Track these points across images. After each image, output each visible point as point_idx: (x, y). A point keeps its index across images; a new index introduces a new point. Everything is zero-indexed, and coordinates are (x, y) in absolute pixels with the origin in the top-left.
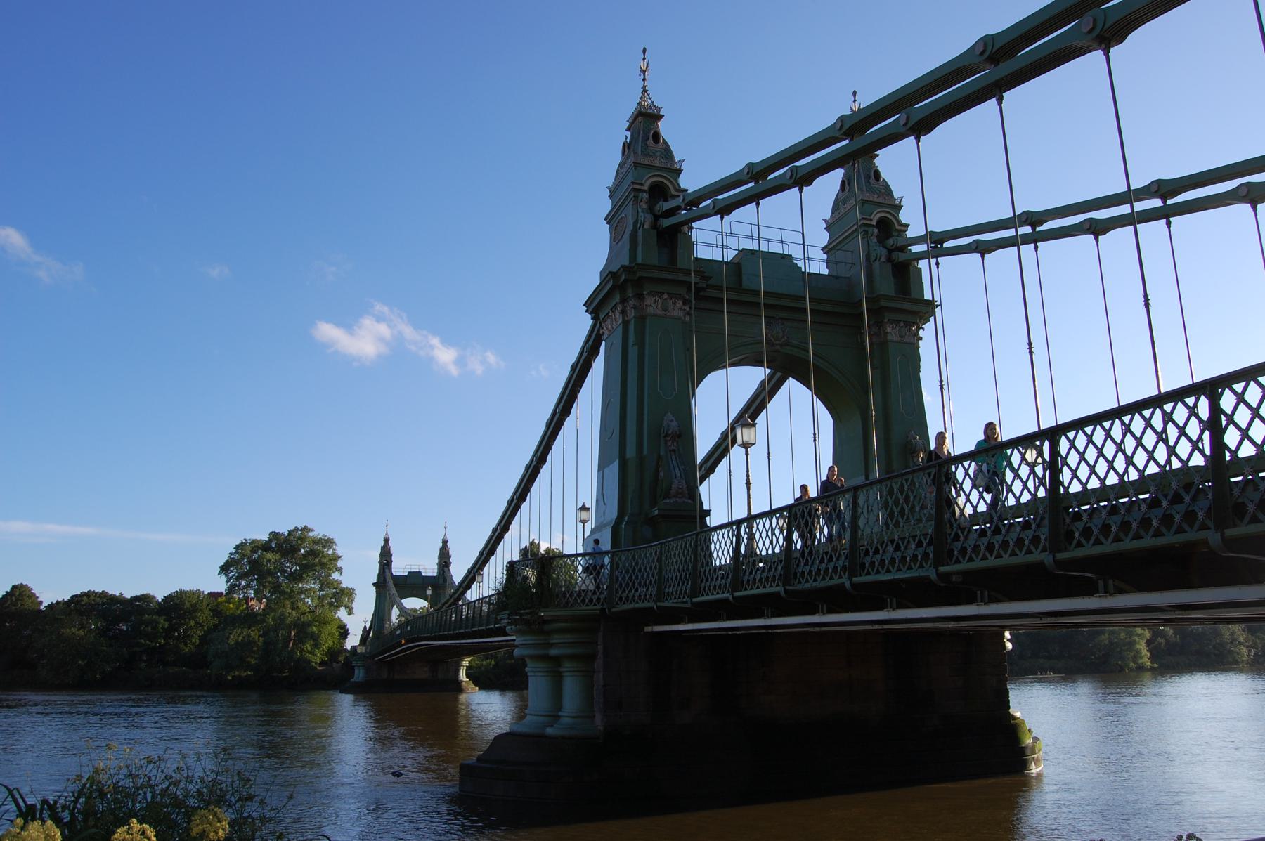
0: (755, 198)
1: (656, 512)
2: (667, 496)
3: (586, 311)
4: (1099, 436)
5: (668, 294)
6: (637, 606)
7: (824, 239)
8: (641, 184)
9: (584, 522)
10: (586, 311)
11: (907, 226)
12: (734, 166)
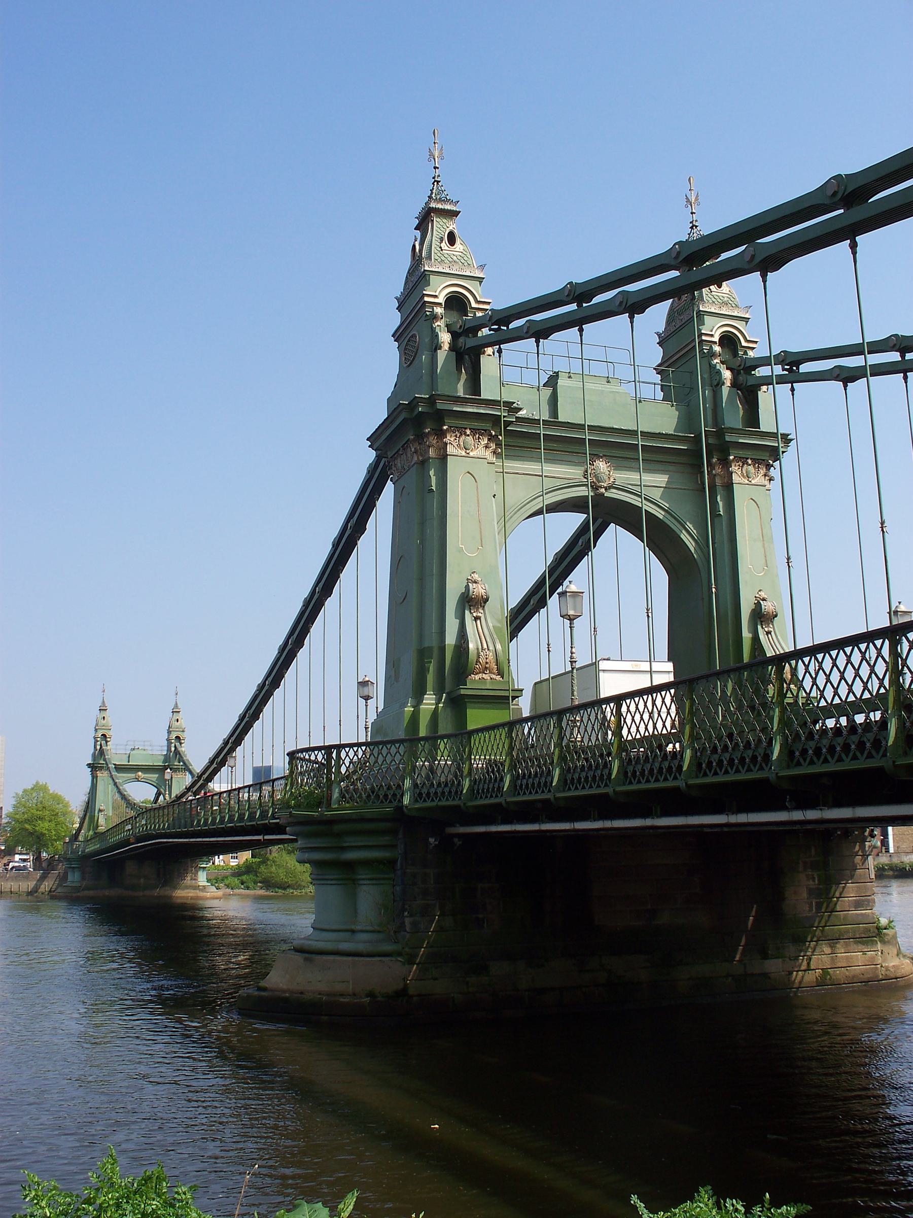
0: (578, 322)
3: (369, 447)
6: (440, 803)
7: (657, 355)
8: (436, 296)
9: (367, 698)
10: (369, 447)
12: (553, 284)
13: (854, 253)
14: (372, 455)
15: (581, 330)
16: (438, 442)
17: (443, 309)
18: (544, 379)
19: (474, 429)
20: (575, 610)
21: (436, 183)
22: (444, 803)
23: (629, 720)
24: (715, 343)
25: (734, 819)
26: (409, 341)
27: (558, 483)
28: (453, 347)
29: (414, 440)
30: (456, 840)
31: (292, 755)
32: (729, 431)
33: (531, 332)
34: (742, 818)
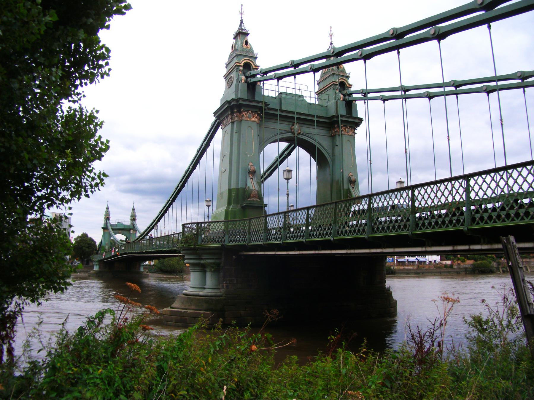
1: (245, 204)
2: (249, 197)
3: (214, 116)
4: (429, 190)
8: (240, 63)
9: (209, 206)
11: (352, 85)
12: (286, 60)
13: (399, 55)
14: (214, 119)
15: (295, 77)
22: (239, 243)
24: (337, 85)
25: (349, 251)
28: (246, 81)
29: (230, 114)
30: (242, 257)
31: (184, 226)
33: (276, 77)
34: (352, 251)
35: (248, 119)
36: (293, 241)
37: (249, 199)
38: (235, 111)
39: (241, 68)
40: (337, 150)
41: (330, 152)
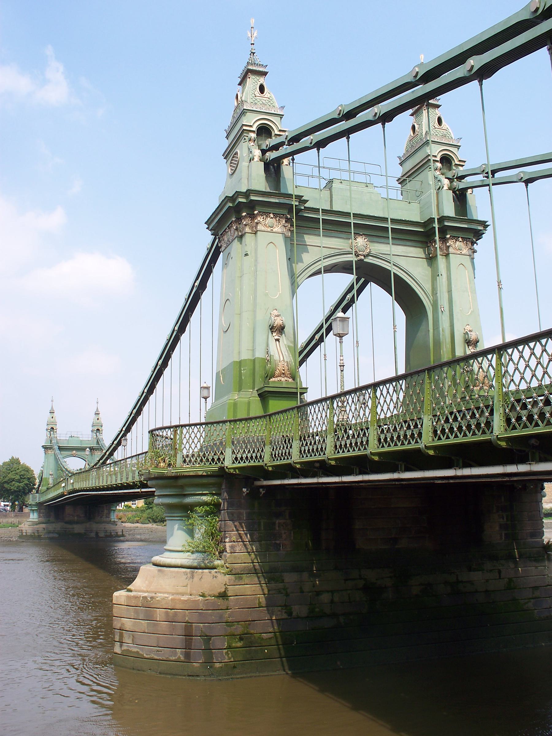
0: (346, 133)
2: (273, 376)
5: (273, 214)
8: (251, 126)
9: (206, 398)
16: (251, 222)
17: (256, 135)
18: (324, 183)
19: (276, 214)
20: (343, 330)
21: (252, 54)
22: (252, 463)
23: (382, 401)
24: (437, 161)
26: (233, 157)
27: (332, 252)
29: (235, 221)
30: (261, 490)
31: (151, 432)
32: (447, 218)
34: (467, 472)
35: (269, 230)
36: (354, 454)
37: (273, 379)
38: (244, 214)
39: (253, 135)
40: (442, 281)
41: (428, 287)
